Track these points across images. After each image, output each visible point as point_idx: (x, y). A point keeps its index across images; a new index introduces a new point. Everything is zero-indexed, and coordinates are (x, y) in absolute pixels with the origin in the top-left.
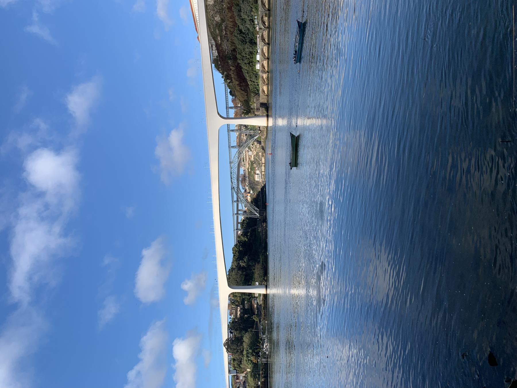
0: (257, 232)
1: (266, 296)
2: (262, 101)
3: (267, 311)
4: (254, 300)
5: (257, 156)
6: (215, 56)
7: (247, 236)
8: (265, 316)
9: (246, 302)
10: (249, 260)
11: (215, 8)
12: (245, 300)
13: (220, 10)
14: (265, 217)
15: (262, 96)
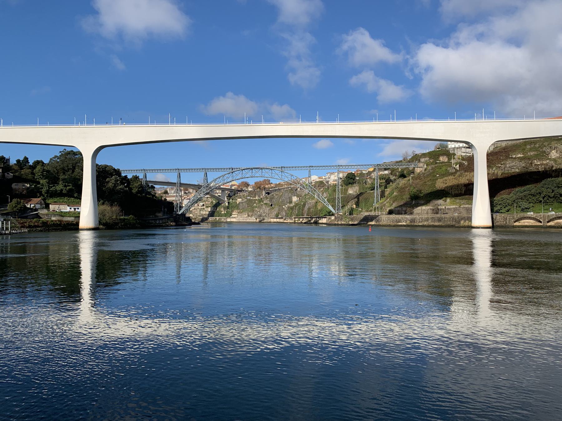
1: (74, 227)
2: (498, 217)
3: (41, 231)
4: (41, 204)
6: (454, 150)
7: (139, 192)
8: (30, 227)
9: (28, 186)
10: (119, 192)
12: (31, 184)
14: (180, 223)
15: (513, 216)
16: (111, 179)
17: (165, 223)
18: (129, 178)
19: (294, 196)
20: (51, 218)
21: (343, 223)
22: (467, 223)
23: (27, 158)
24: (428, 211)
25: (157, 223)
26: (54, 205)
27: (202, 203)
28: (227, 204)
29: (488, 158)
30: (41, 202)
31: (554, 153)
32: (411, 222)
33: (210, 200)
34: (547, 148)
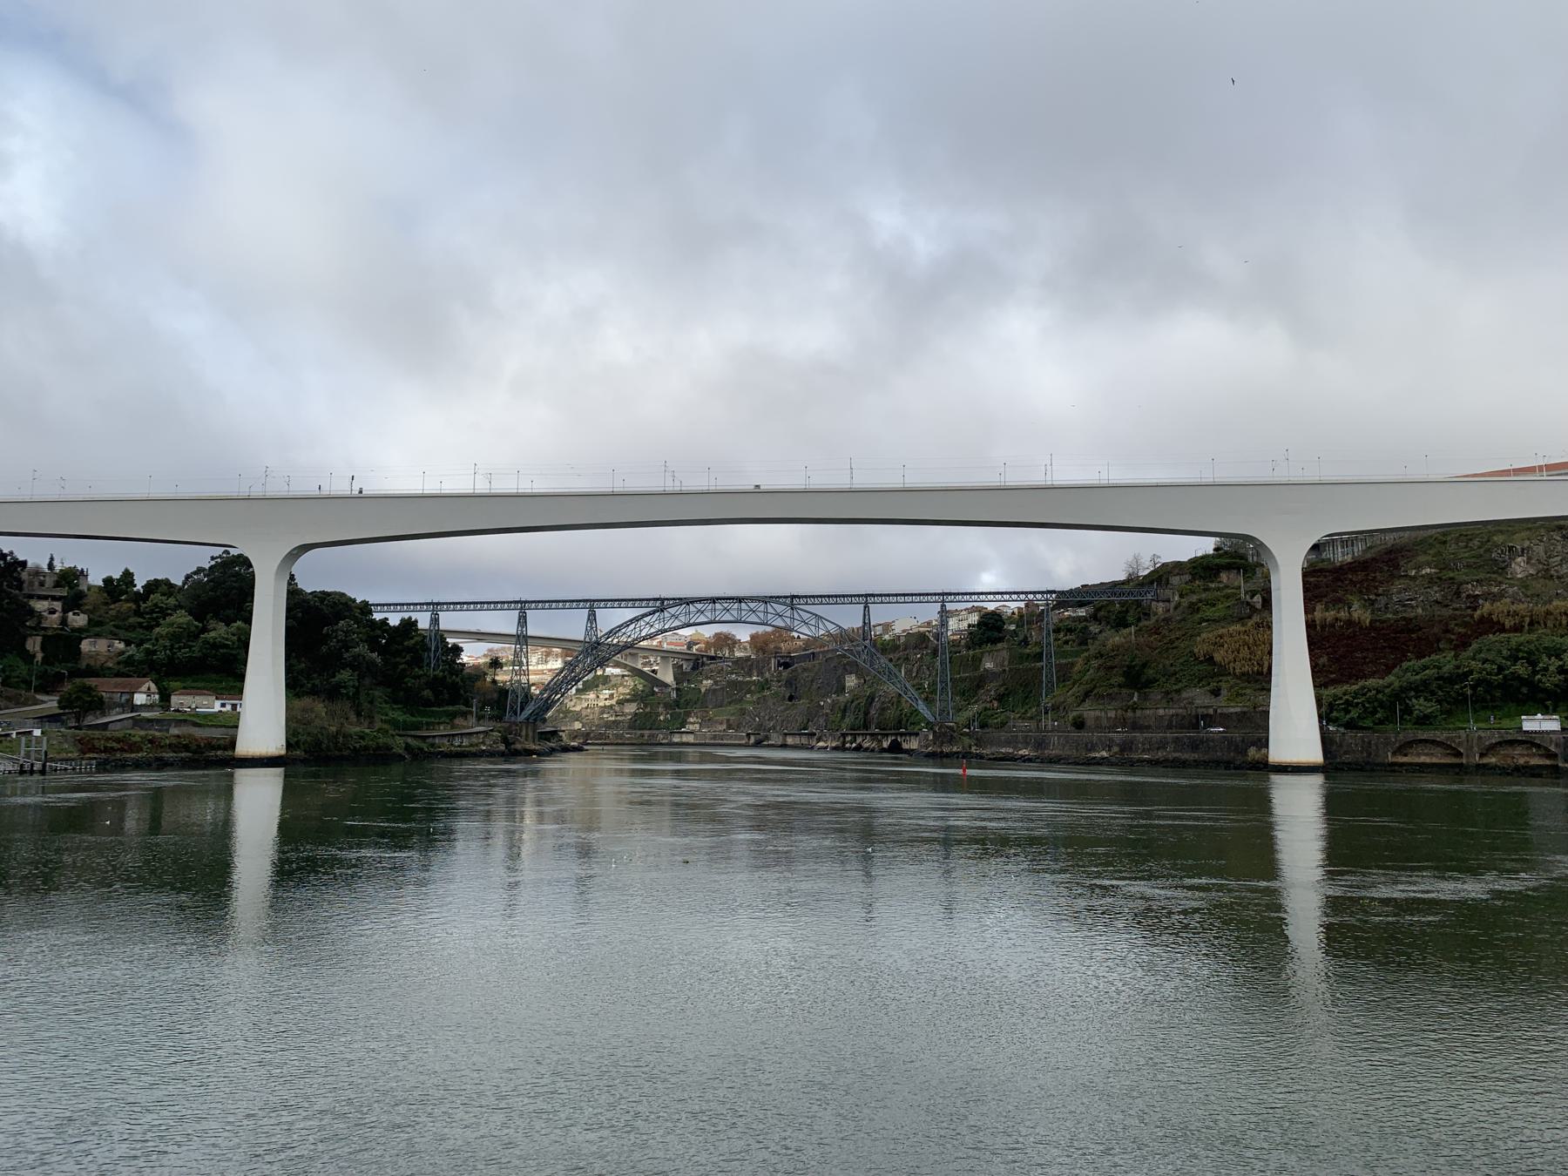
0: (450, 708)
5: (561, 715)
11: (1559, 558)
13: (1558, 578)
16: (335, 628)
17: (477, 745)
18: (392, 624)
19: (851, 673)
20: (167, 731)
21: (955, 749)
22: (1252, 753)
23: (132, 574)
24: (1170, 721)
25: (455, 747)
26: (182, 697)
27: (607, 691)
28: (674, 695)
29: (1306, 579)
30: (149, 689)
31: (1522, 564)
32: (1122, 750)
33: (630, 682)
34: (1502, 551)
